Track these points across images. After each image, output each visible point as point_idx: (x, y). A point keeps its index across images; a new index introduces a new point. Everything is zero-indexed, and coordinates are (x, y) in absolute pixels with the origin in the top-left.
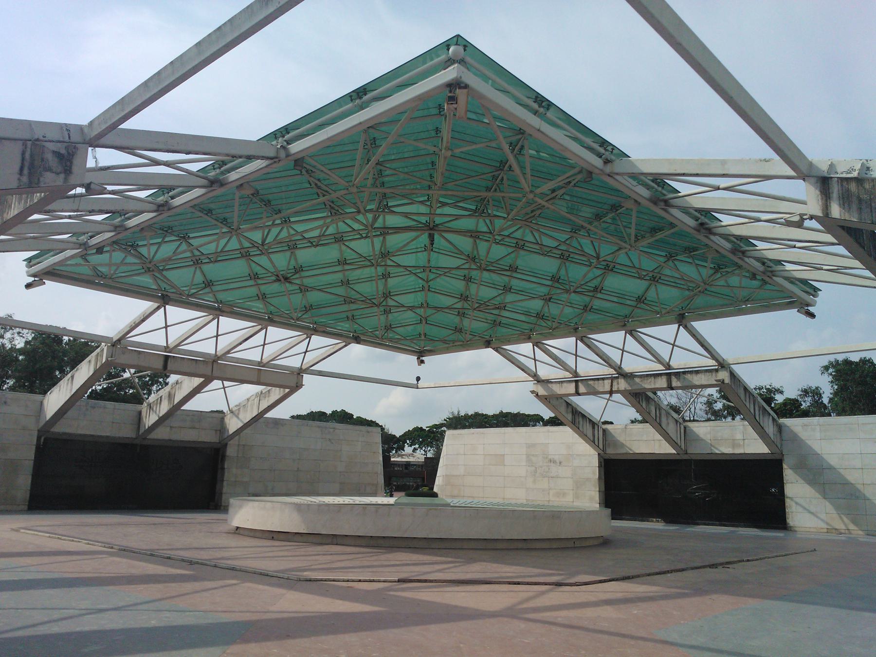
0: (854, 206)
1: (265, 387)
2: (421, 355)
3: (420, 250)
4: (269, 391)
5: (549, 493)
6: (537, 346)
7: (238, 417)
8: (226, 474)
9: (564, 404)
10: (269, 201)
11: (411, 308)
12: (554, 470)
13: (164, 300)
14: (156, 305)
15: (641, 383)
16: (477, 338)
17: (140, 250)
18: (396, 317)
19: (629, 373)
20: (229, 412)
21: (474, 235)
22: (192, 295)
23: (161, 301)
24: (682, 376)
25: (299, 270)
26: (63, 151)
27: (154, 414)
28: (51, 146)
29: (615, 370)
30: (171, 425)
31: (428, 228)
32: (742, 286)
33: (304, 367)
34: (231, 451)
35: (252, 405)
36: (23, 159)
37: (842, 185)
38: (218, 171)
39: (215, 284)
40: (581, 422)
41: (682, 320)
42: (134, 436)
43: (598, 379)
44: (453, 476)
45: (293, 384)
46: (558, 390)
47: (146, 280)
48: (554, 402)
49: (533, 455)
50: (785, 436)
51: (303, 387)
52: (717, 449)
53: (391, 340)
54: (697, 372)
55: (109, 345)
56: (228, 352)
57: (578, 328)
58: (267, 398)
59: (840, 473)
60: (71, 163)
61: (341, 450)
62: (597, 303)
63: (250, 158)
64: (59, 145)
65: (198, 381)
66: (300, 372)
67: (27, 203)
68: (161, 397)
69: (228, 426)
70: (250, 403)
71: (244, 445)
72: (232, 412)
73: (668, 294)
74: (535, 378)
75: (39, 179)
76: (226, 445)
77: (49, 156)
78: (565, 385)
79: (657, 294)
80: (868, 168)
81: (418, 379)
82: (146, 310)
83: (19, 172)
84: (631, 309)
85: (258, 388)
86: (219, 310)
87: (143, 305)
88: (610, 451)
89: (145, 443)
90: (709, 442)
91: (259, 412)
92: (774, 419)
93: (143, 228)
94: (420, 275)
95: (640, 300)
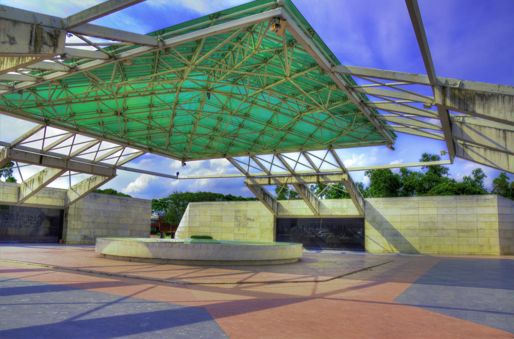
0: (457, 101)
1: (92, 175)
2: (184, 160)
3: (196, 101)
4: (95, 178)
5: (246, 236)
6: (252, 158)
7: (76, 192)
8: (68, 224)
9: (260, 190)
10: (124, 69)
11: (185, 134)
12: (250, 224)
13: (47, 122)
14: (41, 125)
15: (303, 179)
16: (219, 152)
17: (38, 93)
19: (297, 174)
20: (70, 189)
21: (231, 95)
22: (65, 121)
23: (45, 123)
24: (325, 176)
25: (126, 109)
26: (53, 33)
27: (29, 189)
28: (47, 30)
29: (291, 172)
30: (37, 196)
31: (207, 90)
32: (365, 132)
33: (117, 165)
34: (71, 211)
35: (85, 186)
36: (31, 36)
37: (452, 91)
38: (113, 51)
39: (76, 115)
40: (267, 199)
41: (330, 148)
42: (16, 202)
43: (281, 177)
44: (192, 227)
45: (111, 174)
46: (258, 181)
47: (37, 111)
48: (256, 188)
49: (239, 216)
50: (366, 207)
51: (117, 176)
52: (334, 213)
53: (169, 151)
54: (332, 174)
55: (8, 148)
56: (77, 155)
57: (276, 149)
58: (94, 182)
59: (390, 225)
60: (57, 41)
61: (131, 212)
62: (290, 136)
63: (137, 45)
64: (51, 29)
65: (57, 171)
66: (115, 168)
67: (19, 62)
68: (33, 179)
69: (69, 197)
70: (83, 185)
71: (78, 208)
72: (72, 189)
73: (325, 134)
74: (247, 175)
75: (40, 49)
76: (68, 207)
77: (46, 35)
78: (263, 179)
79: (322, 134)
80: (463, 84)
81: (178, 174)
82: (33, 129)
83: (29, 43)
84: (306, 140)
85: (89, 176)
86: (76, 130)
87: (34, 125)
88: (281, 214)
89: (22, 205)
90: (330, 209)
91: (90, 188)
92: (363, 199)
93: (52, 81)
94: (195, 115)
95: (311, 136)
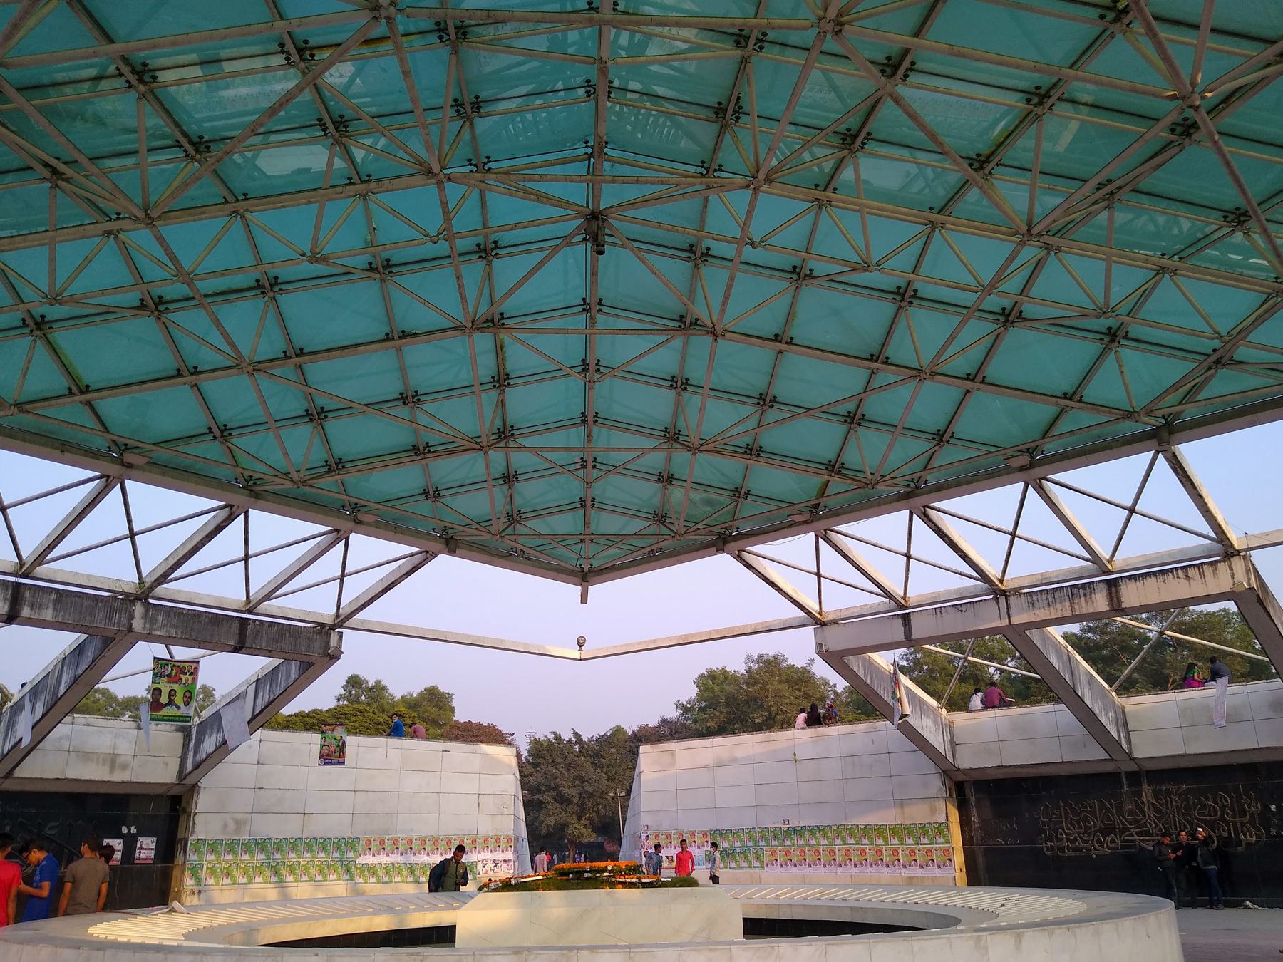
18: (529, 493)
